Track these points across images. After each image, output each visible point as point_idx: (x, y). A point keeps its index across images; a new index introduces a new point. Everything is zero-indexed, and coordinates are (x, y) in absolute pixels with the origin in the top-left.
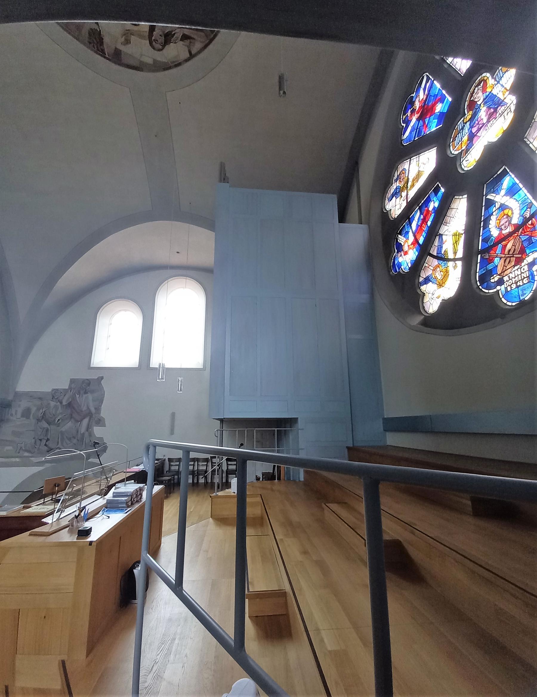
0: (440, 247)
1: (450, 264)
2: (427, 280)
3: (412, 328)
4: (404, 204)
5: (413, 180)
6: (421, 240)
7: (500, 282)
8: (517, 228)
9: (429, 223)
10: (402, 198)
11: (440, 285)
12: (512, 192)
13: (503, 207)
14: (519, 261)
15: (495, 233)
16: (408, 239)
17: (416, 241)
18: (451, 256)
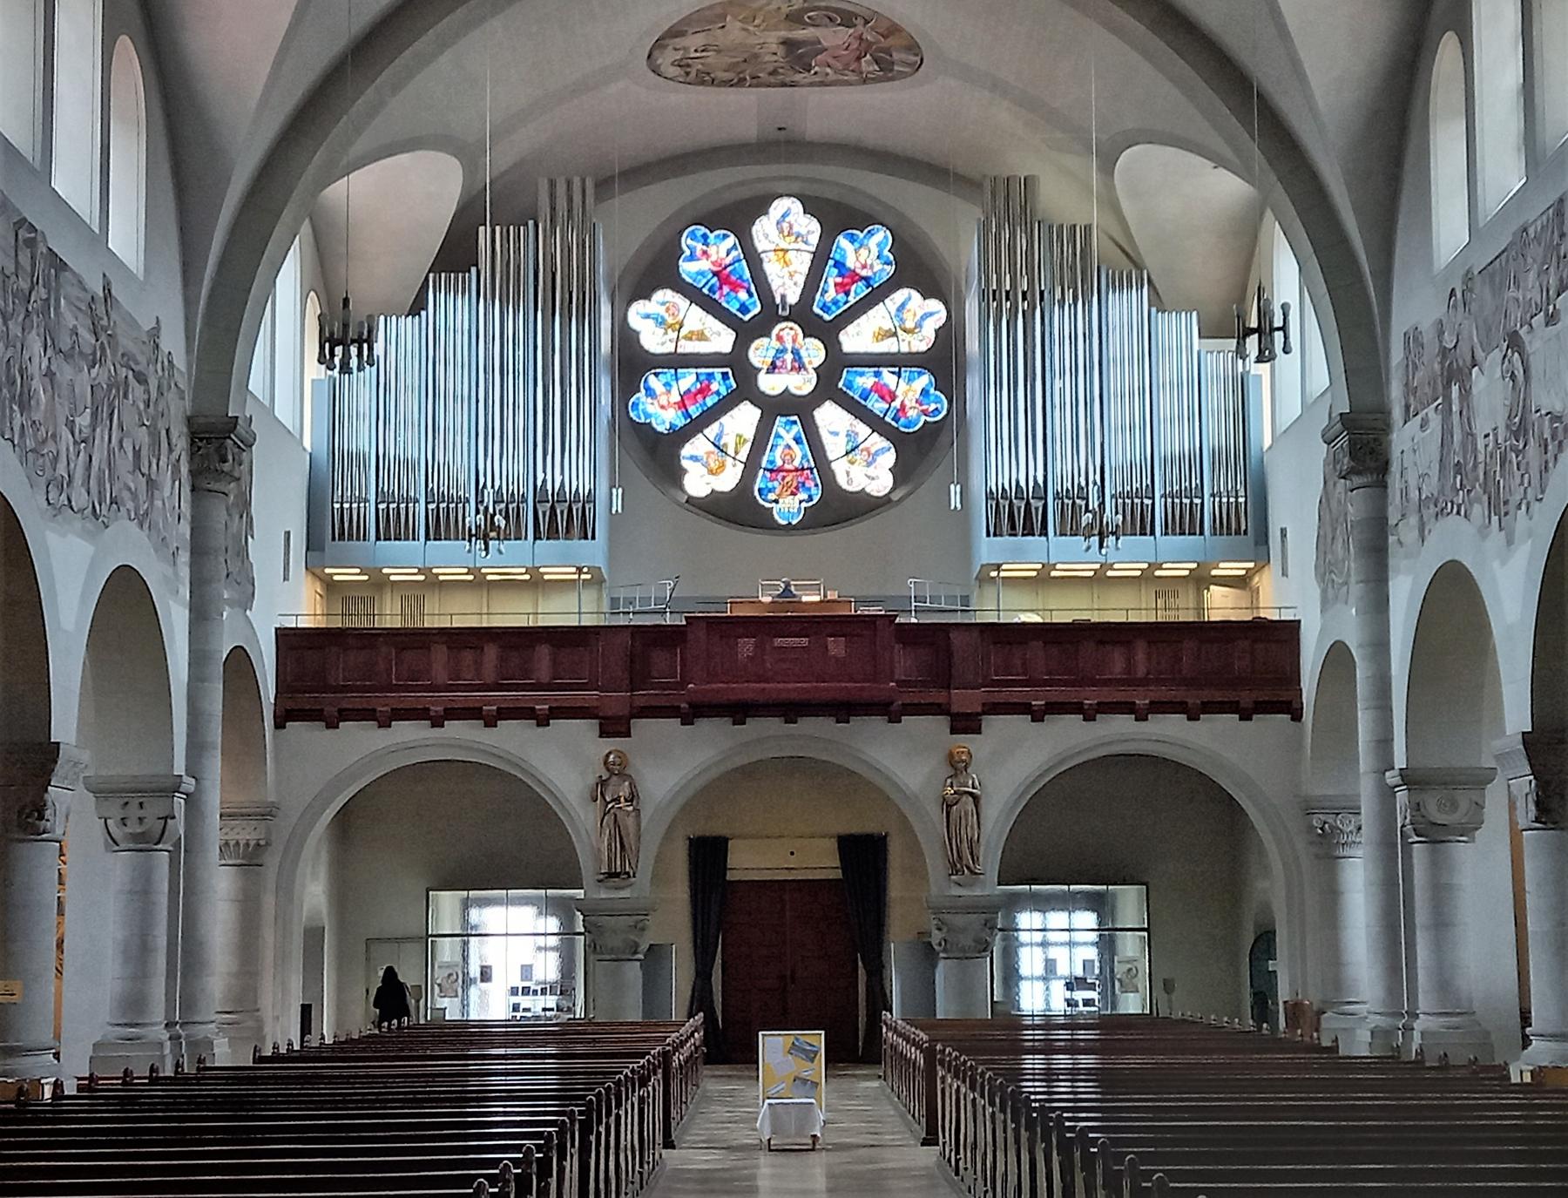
0: (719, 436)
1: (729, 461)
2: (694, 458)
3: (680, 505)
4: (670, 348)
5: (692, 332)
6: (694, 411)
7: (776, 501)
8: (797, 470)
9: (710, 401)
10: (667, 337)
11: (711, 472)
12: (797, 440)
13: (789, 447)
14: (793, 494)
15: (779, 463)
16: (669, 392)
17: (682, 405)
18: (731, 451)
